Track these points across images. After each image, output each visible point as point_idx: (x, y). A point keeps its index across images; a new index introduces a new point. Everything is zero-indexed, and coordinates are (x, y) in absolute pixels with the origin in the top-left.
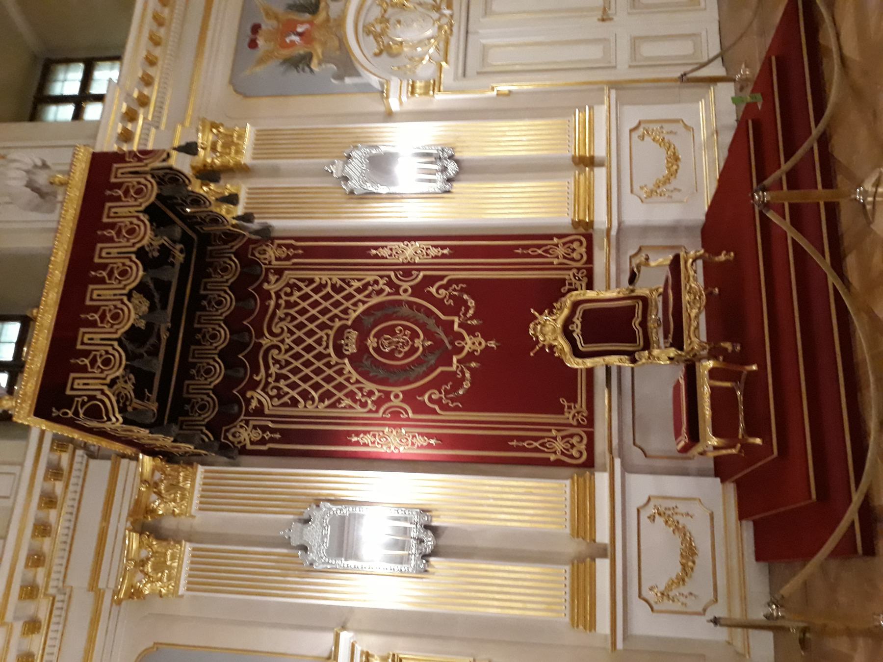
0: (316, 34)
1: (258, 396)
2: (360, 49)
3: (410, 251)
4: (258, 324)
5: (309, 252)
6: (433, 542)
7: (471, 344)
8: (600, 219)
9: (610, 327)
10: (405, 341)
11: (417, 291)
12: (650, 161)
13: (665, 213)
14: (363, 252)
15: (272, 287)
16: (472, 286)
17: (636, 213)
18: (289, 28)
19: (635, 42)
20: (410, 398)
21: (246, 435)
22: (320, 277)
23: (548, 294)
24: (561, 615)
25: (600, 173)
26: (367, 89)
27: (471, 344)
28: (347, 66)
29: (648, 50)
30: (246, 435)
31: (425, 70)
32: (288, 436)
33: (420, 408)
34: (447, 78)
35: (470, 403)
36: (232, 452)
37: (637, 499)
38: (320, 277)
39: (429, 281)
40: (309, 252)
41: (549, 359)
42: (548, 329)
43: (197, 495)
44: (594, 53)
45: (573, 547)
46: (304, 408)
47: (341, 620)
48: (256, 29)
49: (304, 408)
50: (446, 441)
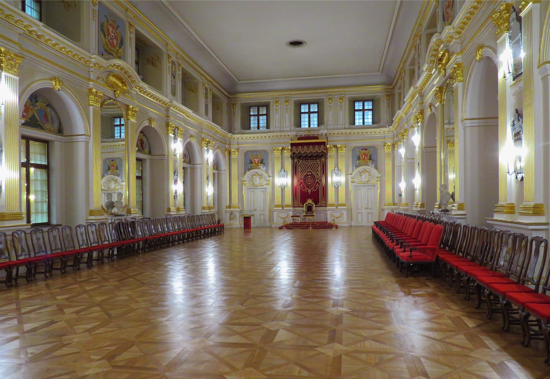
0: (364, 161)
1: (301, 161)
2: (360, 169)
3: (324, 181)
4: (312, 159)
5: (323, 165)
6: (283, 189)
7: (309, 191)
8: (328, 208)
9: (309, 209)
10: (310, 181)
11: (317, 182)
12: (337, 214)
13: (329, 217)
14: (323, 173)
15: (318, 161)
16: (318, 190)
17: (329, 213)
18: (366, 155)
19: (361, 213)
20: (301, 183)
21: (296, 160)
22: (319, 167)
23: (316, 201)
24: (276, 203)
25: (335, 208)
26: (353, 170)
27: (309, 191)
28: (357, 167)
29: (360, 215)
30: (296, 160)
31: (356, 180)
32: (296, 166)
33: (300, 184)
34: (354, 184)
35: (301, 191)
36: (293, 158)
37: (289, 212)
38: (319, 167)
39: (319, 184)
40: (323, 165)
41: (306, 201)
42: (310, 201)
43: (287, 154)
44: (360, 206)
45: (284, 205)
46: (300, 168)
47: (273, 177)
48: (366, 149)
49: (300, 168)
50: (296, 188)
